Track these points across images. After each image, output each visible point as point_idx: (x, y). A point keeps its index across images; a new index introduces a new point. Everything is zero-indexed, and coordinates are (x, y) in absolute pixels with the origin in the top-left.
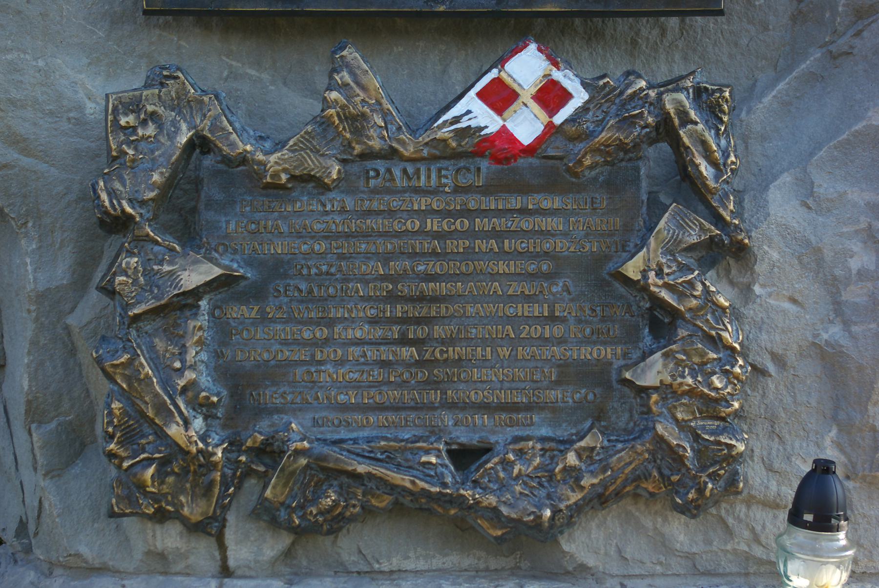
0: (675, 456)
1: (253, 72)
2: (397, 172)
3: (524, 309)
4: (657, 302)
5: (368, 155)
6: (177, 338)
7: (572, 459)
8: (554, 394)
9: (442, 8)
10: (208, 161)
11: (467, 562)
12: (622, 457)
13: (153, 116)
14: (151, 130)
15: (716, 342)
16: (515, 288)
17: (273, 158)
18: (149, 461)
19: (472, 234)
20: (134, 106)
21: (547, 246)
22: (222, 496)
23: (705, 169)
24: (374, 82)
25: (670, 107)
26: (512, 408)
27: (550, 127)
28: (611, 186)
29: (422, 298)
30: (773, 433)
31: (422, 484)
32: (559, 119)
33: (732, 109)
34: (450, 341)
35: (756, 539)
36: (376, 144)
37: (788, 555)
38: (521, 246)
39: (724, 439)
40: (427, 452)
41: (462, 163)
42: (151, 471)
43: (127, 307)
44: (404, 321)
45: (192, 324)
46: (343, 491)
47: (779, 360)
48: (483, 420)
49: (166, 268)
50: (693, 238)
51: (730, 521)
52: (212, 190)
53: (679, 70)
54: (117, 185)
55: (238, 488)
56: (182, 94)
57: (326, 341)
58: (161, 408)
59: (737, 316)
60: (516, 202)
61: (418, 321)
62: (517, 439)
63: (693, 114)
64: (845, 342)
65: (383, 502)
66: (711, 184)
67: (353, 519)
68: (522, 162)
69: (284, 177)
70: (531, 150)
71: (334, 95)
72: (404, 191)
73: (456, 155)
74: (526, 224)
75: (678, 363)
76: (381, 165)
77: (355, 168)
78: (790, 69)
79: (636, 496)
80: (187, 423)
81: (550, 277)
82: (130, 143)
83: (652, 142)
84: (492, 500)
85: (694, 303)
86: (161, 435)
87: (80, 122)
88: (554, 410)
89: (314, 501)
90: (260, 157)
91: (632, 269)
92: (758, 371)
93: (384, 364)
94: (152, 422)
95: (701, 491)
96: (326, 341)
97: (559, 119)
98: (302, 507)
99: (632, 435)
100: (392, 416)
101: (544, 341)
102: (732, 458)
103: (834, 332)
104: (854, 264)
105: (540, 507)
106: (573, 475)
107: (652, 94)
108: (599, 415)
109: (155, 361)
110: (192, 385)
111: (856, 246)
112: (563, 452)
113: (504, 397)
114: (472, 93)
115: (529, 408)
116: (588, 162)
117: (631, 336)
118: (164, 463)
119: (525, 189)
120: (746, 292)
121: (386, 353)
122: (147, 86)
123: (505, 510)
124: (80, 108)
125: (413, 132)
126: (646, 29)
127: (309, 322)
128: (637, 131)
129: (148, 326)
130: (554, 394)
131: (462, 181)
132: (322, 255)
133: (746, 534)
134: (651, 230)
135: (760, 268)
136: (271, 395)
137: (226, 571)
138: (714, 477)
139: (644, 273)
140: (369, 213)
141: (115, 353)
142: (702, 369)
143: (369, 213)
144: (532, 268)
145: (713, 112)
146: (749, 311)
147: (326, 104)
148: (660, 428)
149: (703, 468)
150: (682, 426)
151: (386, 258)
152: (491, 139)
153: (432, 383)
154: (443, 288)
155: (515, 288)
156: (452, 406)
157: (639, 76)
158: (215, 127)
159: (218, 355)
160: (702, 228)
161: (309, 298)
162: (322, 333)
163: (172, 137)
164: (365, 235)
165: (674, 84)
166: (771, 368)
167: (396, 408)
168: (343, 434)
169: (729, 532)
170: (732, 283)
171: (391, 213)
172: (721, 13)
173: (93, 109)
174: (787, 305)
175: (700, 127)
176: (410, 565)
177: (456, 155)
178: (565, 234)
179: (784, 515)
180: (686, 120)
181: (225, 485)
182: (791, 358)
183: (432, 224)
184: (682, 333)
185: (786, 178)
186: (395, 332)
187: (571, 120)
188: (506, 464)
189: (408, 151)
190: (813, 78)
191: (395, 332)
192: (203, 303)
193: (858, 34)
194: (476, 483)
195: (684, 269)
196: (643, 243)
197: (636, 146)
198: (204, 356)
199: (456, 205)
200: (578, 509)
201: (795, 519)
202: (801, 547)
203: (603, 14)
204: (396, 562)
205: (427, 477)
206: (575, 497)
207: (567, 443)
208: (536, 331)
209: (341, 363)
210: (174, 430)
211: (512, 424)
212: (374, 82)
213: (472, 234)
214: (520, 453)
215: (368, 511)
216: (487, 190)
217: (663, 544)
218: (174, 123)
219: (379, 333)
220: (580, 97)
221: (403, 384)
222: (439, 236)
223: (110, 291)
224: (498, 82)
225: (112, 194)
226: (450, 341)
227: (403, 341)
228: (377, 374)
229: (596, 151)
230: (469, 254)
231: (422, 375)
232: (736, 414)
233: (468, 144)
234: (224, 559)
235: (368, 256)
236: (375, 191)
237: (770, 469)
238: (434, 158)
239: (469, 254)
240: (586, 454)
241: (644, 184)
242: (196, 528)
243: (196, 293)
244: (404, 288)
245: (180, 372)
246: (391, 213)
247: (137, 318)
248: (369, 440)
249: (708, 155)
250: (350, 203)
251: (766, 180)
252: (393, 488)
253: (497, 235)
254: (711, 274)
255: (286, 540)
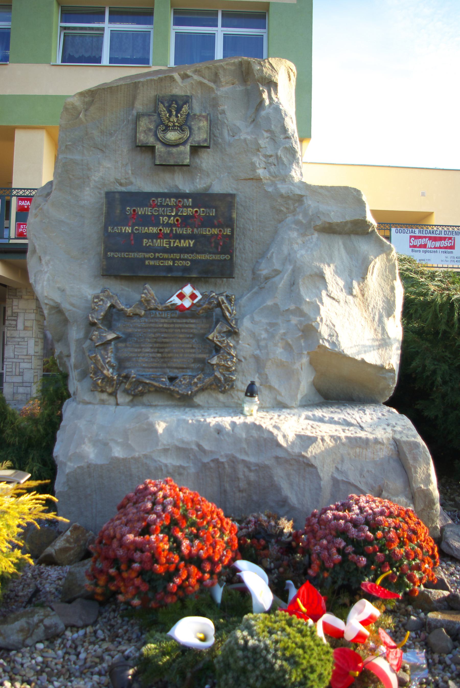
0: (219, 380)
1: (127, 289)
2: (157, 313)
3: (185, 346)
4: (217, 345)
5: (151, 309)
6: (106, 350)
7: (196, 380)
8: (193, 365)
9: (169, 275)
10: (114, 310)
11: (173, 403)
12: (207, 380)
13: (102, 300)
14: (101, 303)
15: (229, 354)
16: (184, 341)
17: (129, 310)
18: (99, 379)
19: (174, 328)
20: (97, 297)
21: (192, 331)
22: (116, 387)
23: (228, 314)
24: (152, 292)
25: (220, 300)
26: (183, 368)
27: (193, 304)
28: (207, 317)
29: (162, 343)
30: (243, 375)
31: (161, 385)
32: (195, 301)
33: (235, 301)
34: (169, 353)
35: (239, 399)
36: (152, 307)
37: (244, 402)
38: (186, 331)
39: (231, 376)
40: (163, 378)
41: (173, 311)
42: (100, 381)
43: (95, 343)
44: (159, 348)
45: (110, 347)
46: (144, 387)
47: (245, 358)
48: (176, 371)
49: (104, 335)
50: (225, 330)
51: (233, 395)
52: (115, 317)
53: (222, 291)
54: (93, 315)
55: (120, 385)
56: (108, 295)
57: (140, 352)
58: (102, 367)
59: (235, 348)
60: (184, 321)
61: (162, 348)
62: (184, 375)
63: (225, 301)
64: (260, 354)
65: (152, 389)
66: (229, 317)
67: (146, 393)
68: (186, 312)
69: (131, 314)
70: (188, 309)
71: (143, 295)
72: (159, 318)
73: (171, 310)
74: (187, 326)
75: (221, 359)
76: (154, 312)
77: (148, 312)
78: (251, 290)
79: (211, 389)
80: (108, 370)
81: (192, 338)
82: (97, 306)
83: (216, 307)
84: (177, 389)
85: (224, 345)
86: (102, 373)
87: (87, 300)
88: (192, 369)
89: (137, 388)
90: (126, 309)
91: (210, 337)
92: (240, 361)
93: (154, 358)
94: (100, 370)
95: (225, 388)
96: (140, 352)
97: (195, 301)
98: (134, 390)
99: (209, 375)
100: (155, 370)
101: (190, 353)
102: (232, 381)
103: (257, 352)
104: (263, 336)
105: (188, 391)
106: (196, 384)
107: (216, 296)
108: (202, 370)
109: (102, 356)
110: (109, 362)
111: (263, 332)
112: (194, 379)
113: (181, 366)
114: (175, 296)
115: (187, 368)
116: (201, 312)
117: (210, 352)
118: (103, 379)
119: (186, 318)
120: (238, 342)
121: (154, 355)
122: (101, 292)
123: (180, 392)
124: (87, 297)
125: (161, 304)
126: (219, 281)
127: (136, 348)
128: (212, 305)
129: (100, 348)
130: (193, 365)
131: (173, 315)
132: (140, 332)
133: (237, 398)
134: (215, 327)
135: (241, 337)
136: (128, 364)
137: (117, 404)
138: (228, 385)
139: (213, 338)
140: (151, 323)
141: (92, 354)
142: (226, 360)
143: (151, 323)
144: (188, 336)
145: (230, 301)
146: (238, 347)
147: (142, 297)
148: (216, 374)
149: (226, 383)
150: (221, 373)
151: (154, 333)
152: (179, 306)
153: (164, 362)
154: (167, 340)
155: (184, 341)
156: (169, 367)
157: (213, 292)
158: (116, 302)
159: (116, 355)
160: (227, 328)
161: (137, 342)
162: (139, 350)
163: (106, 304)
164: (150, 328)
165: (221, 294)
166: (243, 360)
167: (156, 368)
168: (144, 373)
169: (233, 397)
170: (234, 340)
171: (156, 323)
172: (234, 278)
173: (90, 297)
174: (247, 346)
175: (227, 304)
176: (160, 404)
177: (171, 310)
178: (196, 328)
179: (244, 393)
180: (223, 303)
181: (117, 384)
182: (248, 358)
183: (165, 326)
184: (222, 352)
185: (248, 316)
186: (156, 350)
187: (198, 302)
188: (181, 381)
189: (160, 308)
190: (256, 293)
191: (156, 350)
192: (113, 343)
193: (266, 283)
194: (174, 385)
195: (223, 337)
196: (213, 331)
197: (212, 308)
198: (112, 355)
199: (171, 321)
200: (197, 392)
201: (246, 395)
202: (248, 401)
203: (207, 278)
204: (156, 403)
205: (162, 384)
206: (196, 389)
207: (195, 376)
208: (188, 351)
209: (144, 357)
210: (105, 372)
211: (183, 372)
212: (152, 292)
213: (174, 328)
214: (184, 379)
215: (149, 392)
216: (178, 318)
217: (217, 400)
218: (107, 301)
219: (152, 350)
220: (200, 297)
221: (158, 362)
222: (167, 328)
223: (91, 340)
224: (181, 293)
225: (92, 317)
226: (169, 353)
227: (158, 352)
228: (152, 360)
229: (203, 309)
230: (174, 333)
231: (162, 360)
232: (234, 370)
233: (174, 307)
234: (117, 401)
235: (150, 333)
236: (152, 318)
237: (242, 383)
238: (166, 310)
239: (174, 333)
240: (199, 379)
241: (214, 317)
242: (111, 394)
243: (111, 340)
244: (159, 340)
245: (107, 358)
246: (156, 323)
247: (97, 346)
248: (150, 375)
249: (228, 311)
250: (147, 320)
251: (244, 316)
252: (155, 386)
253: (180, 328)
254: (230, 338)
255: (130, 398)
